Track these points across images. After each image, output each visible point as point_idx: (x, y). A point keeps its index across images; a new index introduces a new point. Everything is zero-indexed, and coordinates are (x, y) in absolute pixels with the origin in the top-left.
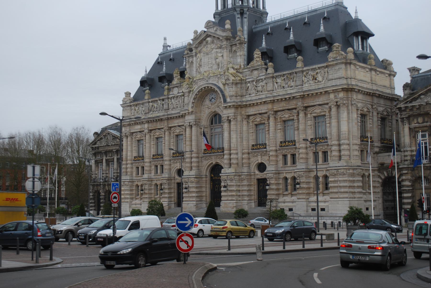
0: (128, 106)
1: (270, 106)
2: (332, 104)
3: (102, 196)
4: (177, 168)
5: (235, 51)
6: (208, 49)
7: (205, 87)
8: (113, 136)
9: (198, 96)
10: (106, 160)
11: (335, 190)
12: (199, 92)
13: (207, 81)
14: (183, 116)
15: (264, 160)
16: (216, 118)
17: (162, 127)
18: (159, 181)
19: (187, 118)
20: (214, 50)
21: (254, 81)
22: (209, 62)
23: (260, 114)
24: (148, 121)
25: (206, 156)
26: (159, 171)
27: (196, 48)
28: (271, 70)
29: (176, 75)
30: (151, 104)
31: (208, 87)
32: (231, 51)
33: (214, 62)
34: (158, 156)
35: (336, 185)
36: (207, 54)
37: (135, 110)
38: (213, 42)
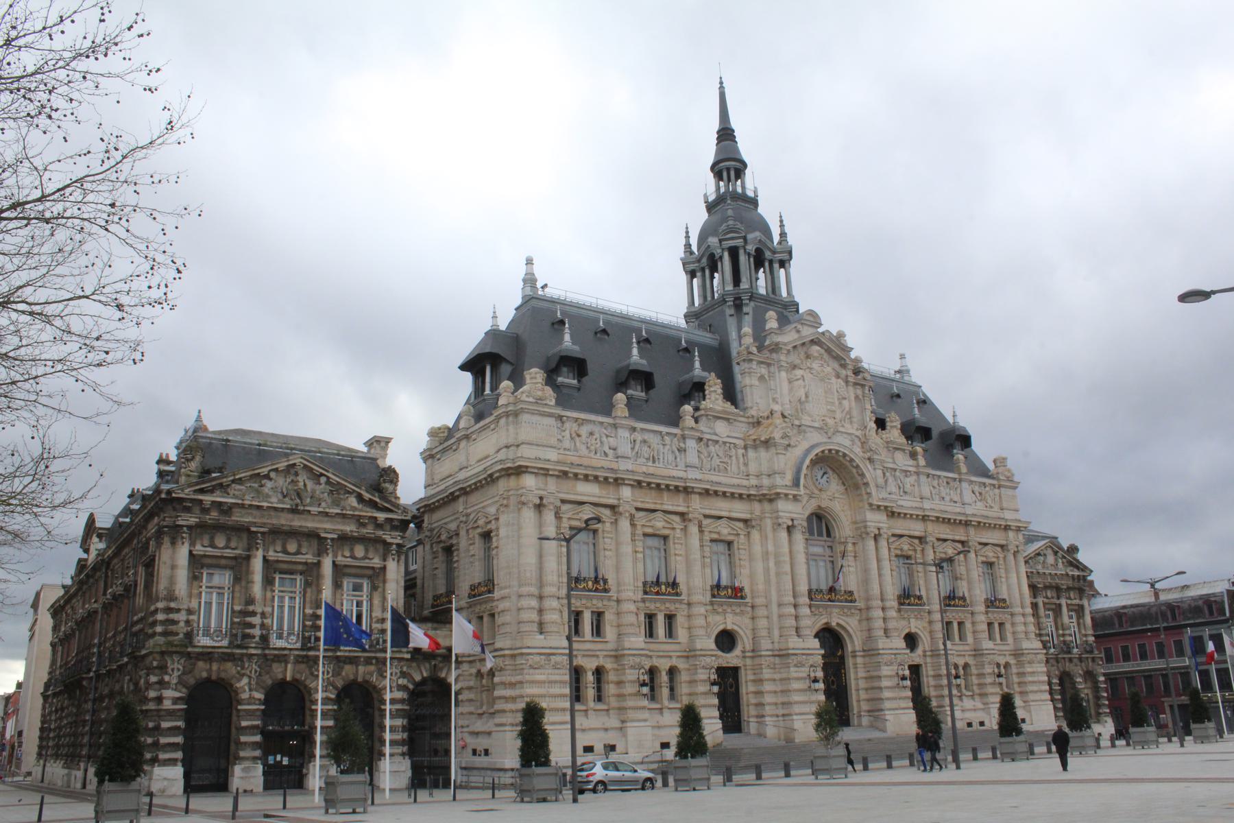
0: (550, 415)
1: (931, 527)
2: (1012, 548)
3: (251, 700)
4: (721, 628)
8: (328, 482)
10: (265, 560)
11: (1035, 688)
14: (771, 498)
15: (915, 626)
16: (820, 523)
17: (681, 509)
18: (663, 660)
19: (781, 505)
23: (910, 537)
24: (639, 482)
25: (818, 607)
26: (661, 629)
28: (922, 462)
30: (638, 437)
34: (662, 586)
35: (1035, 679)
36: (822, 380)
37: (579, 436)
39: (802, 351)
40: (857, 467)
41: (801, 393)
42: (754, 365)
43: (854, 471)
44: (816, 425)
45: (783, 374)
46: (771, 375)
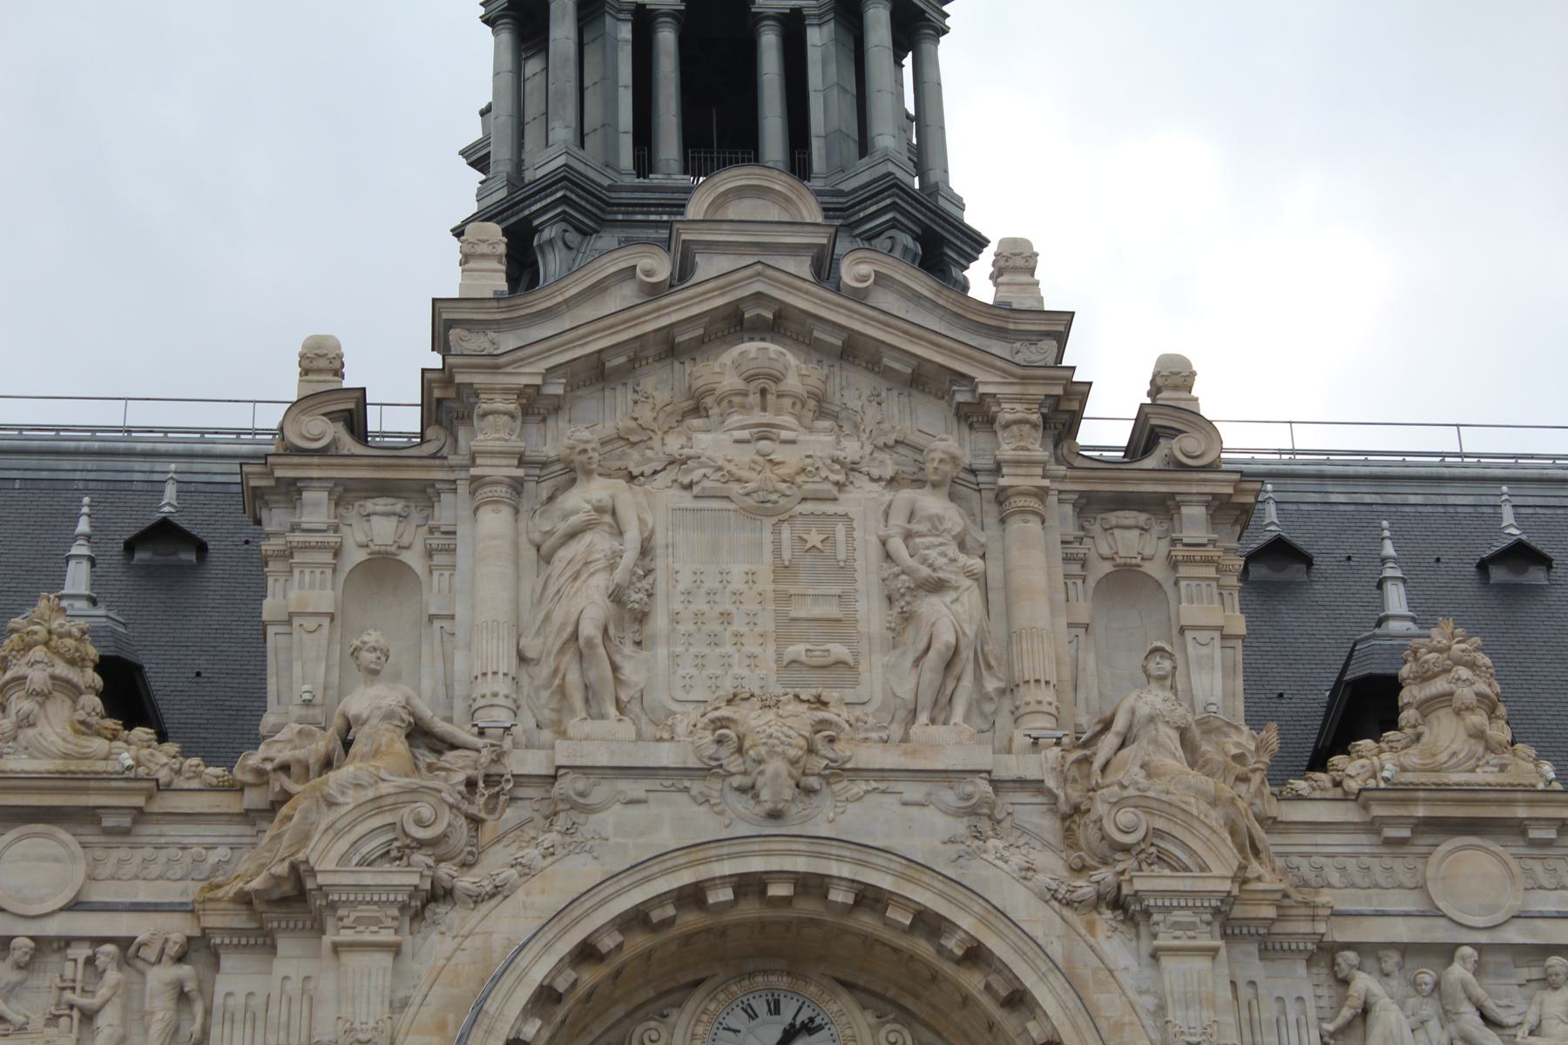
5: (1126, 579)
6: (790, 458)
7: (749, 885)
9: (590, 976)
12: (636, 919)
13: (775, 815)
20: (863, 497)
21: (1447, 952)
22: (785, 598)
27: (534, 406)
29: (62, 669)
31: (812, 885)
32: (1074, 559)
33: (872, 615)
36: (763, 509)
38: (821, 407)
39: (660, 386)
40: (976, 955)
41: (589, 604)
42: (316, 509)
43: (973, 981)
44: (666, 755)
45: (495, 521)
46: (443, 546)
